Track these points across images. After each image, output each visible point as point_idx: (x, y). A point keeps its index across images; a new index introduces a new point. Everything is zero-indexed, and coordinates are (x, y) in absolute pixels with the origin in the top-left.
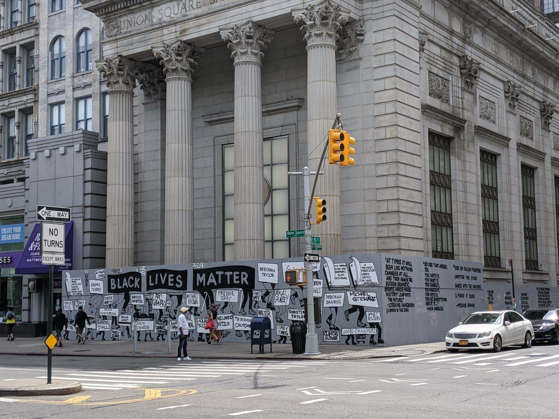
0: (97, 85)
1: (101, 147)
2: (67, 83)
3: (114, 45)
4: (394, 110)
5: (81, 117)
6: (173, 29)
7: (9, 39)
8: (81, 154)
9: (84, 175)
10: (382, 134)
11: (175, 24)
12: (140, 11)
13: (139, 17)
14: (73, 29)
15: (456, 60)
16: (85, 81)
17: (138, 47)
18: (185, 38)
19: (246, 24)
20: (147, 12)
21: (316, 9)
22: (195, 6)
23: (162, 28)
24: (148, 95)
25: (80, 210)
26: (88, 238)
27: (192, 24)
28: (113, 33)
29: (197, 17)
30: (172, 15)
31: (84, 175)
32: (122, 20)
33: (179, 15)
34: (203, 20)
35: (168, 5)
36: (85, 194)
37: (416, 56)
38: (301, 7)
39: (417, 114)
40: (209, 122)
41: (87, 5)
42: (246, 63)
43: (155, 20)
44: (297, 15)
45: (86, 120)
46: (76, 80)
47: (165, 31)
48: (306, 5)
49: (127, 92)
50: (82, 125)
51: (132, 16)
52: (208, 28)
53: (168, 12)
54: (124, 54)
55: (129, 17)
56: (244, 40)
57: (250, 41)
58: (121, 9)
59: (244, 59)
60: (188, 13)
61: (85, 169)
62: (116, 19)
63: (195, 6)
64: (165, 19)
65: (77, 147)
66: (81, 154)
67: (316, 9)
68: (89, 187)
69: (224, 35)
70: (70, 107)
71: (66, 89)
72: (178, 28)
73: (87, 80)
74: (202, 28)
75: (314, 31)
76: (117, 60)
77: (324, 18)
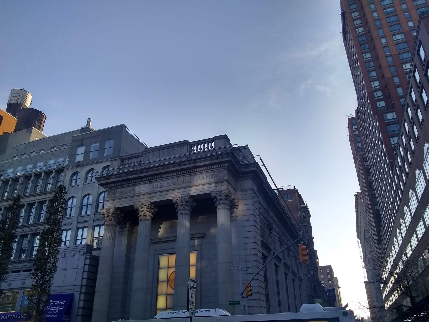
0: (91, 222)
1: (94, 253)
2: (75, 219)
3: (112, 202)
4: (254, 241)
5: (79, 237)
6: (146, 196)
7: (43, 197)
8: (84, 257)
9: (84, 268)
10: (248, 252)
11: (147, 194)
12: (129, 187)
13: (128, 189)
14: (82, 194)
15: (266, 222)
16: (85, 219)
17: (125, 203)
18: (152, 201)
19: (187, 196)
20: (132, 188)
21: (223, 192)
22: (159, 187)
23: (140, 195)
24: (122, 228)
25: (79, 287)
26: (81, 304)
27: (157, 194)
28: (112, 196)
29: (160, 192)
30: (146, 190)
31: (84, 268)
32: (118, 190)
33: (150, 190)
34: (163, 193)
35: (144, 185)
36: (83, 279)
37: (258, 217)
38: (215, 190)
39: (260, 244)
40: (153, 243)
41: (100, 183)
42: (185, 214)
43: (136, 192)
44: (213, 194)
45: (82, 239)
46: (79, 218)
47: (142, 197)
48: (218, 190)
49: (115, 225)
50: (79, 242)
51: (124, 189)
52: (169, 196)
53: (144, 189)
54: (117, 207)
55: (122, 190)
56: (184, 203)
57: (188, 204)
58: (118, 185)
59: (184, 212)
60: (155, 190)
61: (85, 265)
62: (114, 190)
63: (159, 187)
64: (142, 192)
65: (82, 252)
66: (84, 257)
67: (223, 192)
68: (86, 275)
69: (174, 200)
70: (74, 232)
71: (73, 223)
72: (149, 196)
73: (86, 219)
74: (162, 197)
75: (221, 202)
76: (113, 209)
77: (226, 196)
